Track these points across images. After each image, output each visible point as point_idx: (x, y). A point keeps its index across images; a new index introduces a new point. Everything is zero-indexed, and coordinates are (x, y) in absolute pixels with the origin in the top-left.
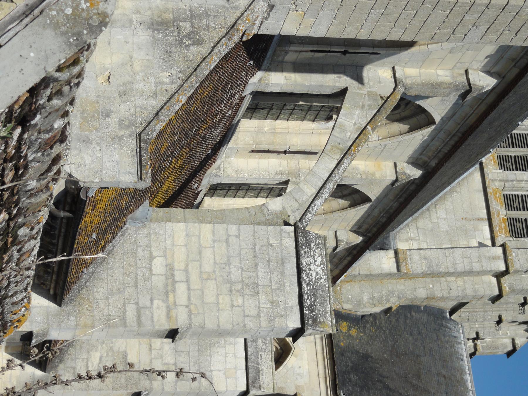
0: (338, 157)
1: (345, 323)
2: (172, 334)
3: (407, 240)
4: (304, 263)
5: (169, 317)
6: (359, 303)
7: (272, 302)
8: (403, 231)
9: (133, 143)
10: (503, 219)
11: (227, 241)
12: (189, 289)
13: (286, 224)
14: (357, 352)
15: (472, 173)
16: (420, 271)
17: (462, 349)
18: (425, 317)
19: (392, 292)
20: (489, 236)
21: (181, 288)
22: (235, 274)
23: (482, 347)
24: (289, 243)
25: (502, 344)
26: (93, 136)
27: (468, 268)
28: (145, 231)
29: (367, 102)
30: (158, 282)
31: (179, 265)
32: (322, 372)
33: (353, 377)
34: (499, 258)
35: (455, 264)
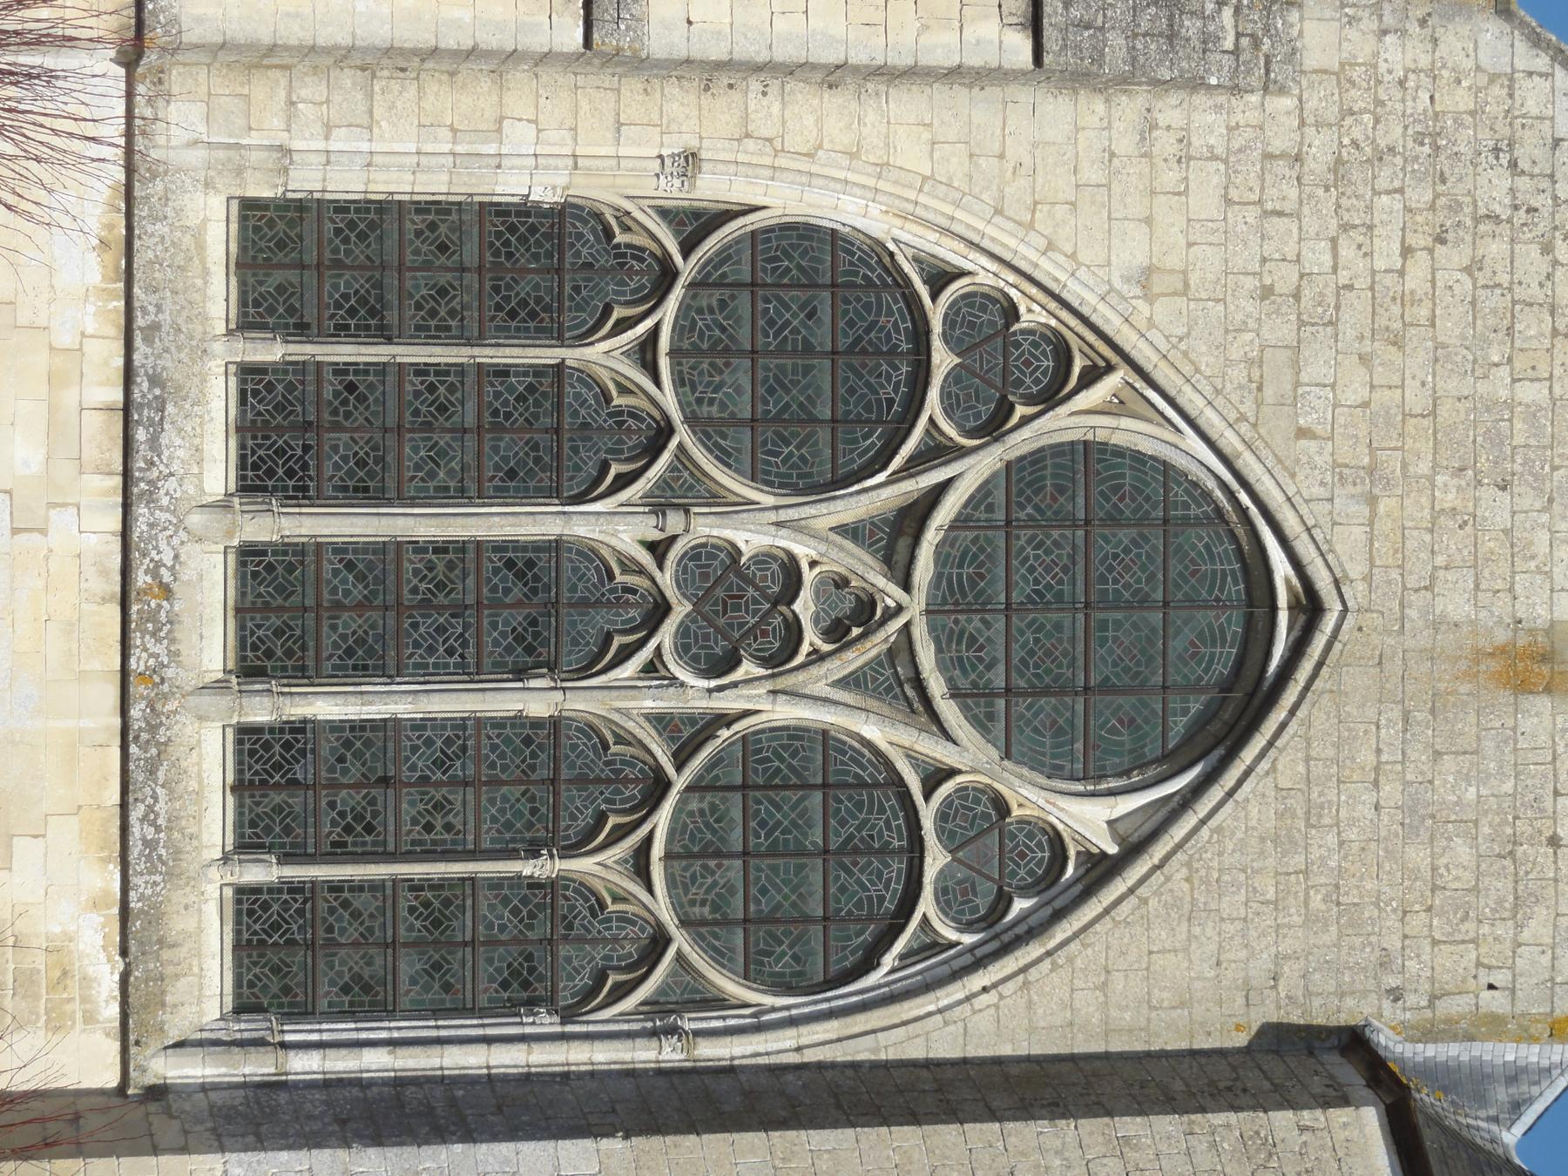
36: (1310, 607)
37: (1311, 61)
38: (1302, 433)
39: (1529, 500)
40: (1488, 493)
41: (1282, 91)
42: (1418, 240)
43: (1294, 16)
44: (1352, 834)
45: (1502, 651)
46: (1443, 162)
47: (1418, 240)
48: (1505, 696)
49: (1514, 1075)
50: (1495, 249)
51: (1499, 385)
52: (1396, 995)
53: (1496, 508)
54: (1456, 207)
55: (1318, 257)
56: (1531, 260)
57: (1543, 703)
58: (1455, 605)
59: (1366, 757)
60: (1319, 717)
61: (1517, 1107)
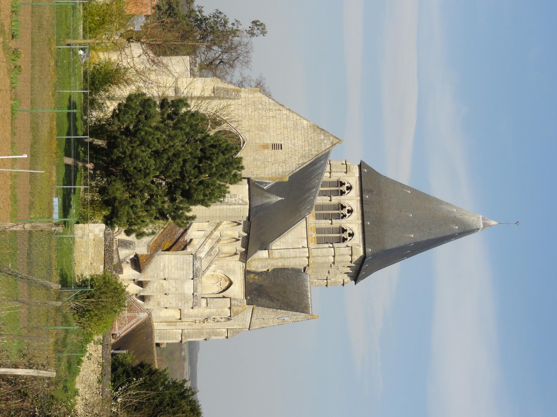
0: (205, 238)
1: (253, 275)
2: (165, 279)
3: (276, 246)
4: (194, 263)
5: (164, 275)
6: (257, 268)
7: (187, 272)
8: (275, 243)
9: (147, 246)
10: (314, 238)
11: (177, 259)
12: (168, 270)
13: (192, 254)
14: (257, 284)
15: (303, 221)
16: (277, 257)
17: (308, 283)
18: (291, 272)
19: (269, 264)
20: (306, 244)
21: (167, 270)
22: (179, 266)
23: (330, 283)
24: (192, 259)
25: (339, 282)
26: (140, 245)
27: (295, 256)
28: (159, 257)
29: (214, 224)
30: (162, 268)
31: (166, 264)
32: (242, 290)
33: (254, 292)
34: (306, 252)
35: (290, 254)
36: (244, 143)
37: (242, 97)
38: (242, 127)
39: (264, 132)
40: (260, 132)
41: (240, 99)
42: (253, 111)
43: (241, 93)
44: (248, 161)
45: (262, 145)
46: (255, 104)
47: (253, 111)
48: (263, 149)
49: (266, 183)
50: (260, 112)
51: (261, 123)
52: (253, 175)
53: (261, 133)
54: (256, 108)
55: (243, 113)
56: (264, 112)
57: (267, 150)
58: (258, 141)
59: (250, 154)
60: (245, 151)
61: (266, 186)
